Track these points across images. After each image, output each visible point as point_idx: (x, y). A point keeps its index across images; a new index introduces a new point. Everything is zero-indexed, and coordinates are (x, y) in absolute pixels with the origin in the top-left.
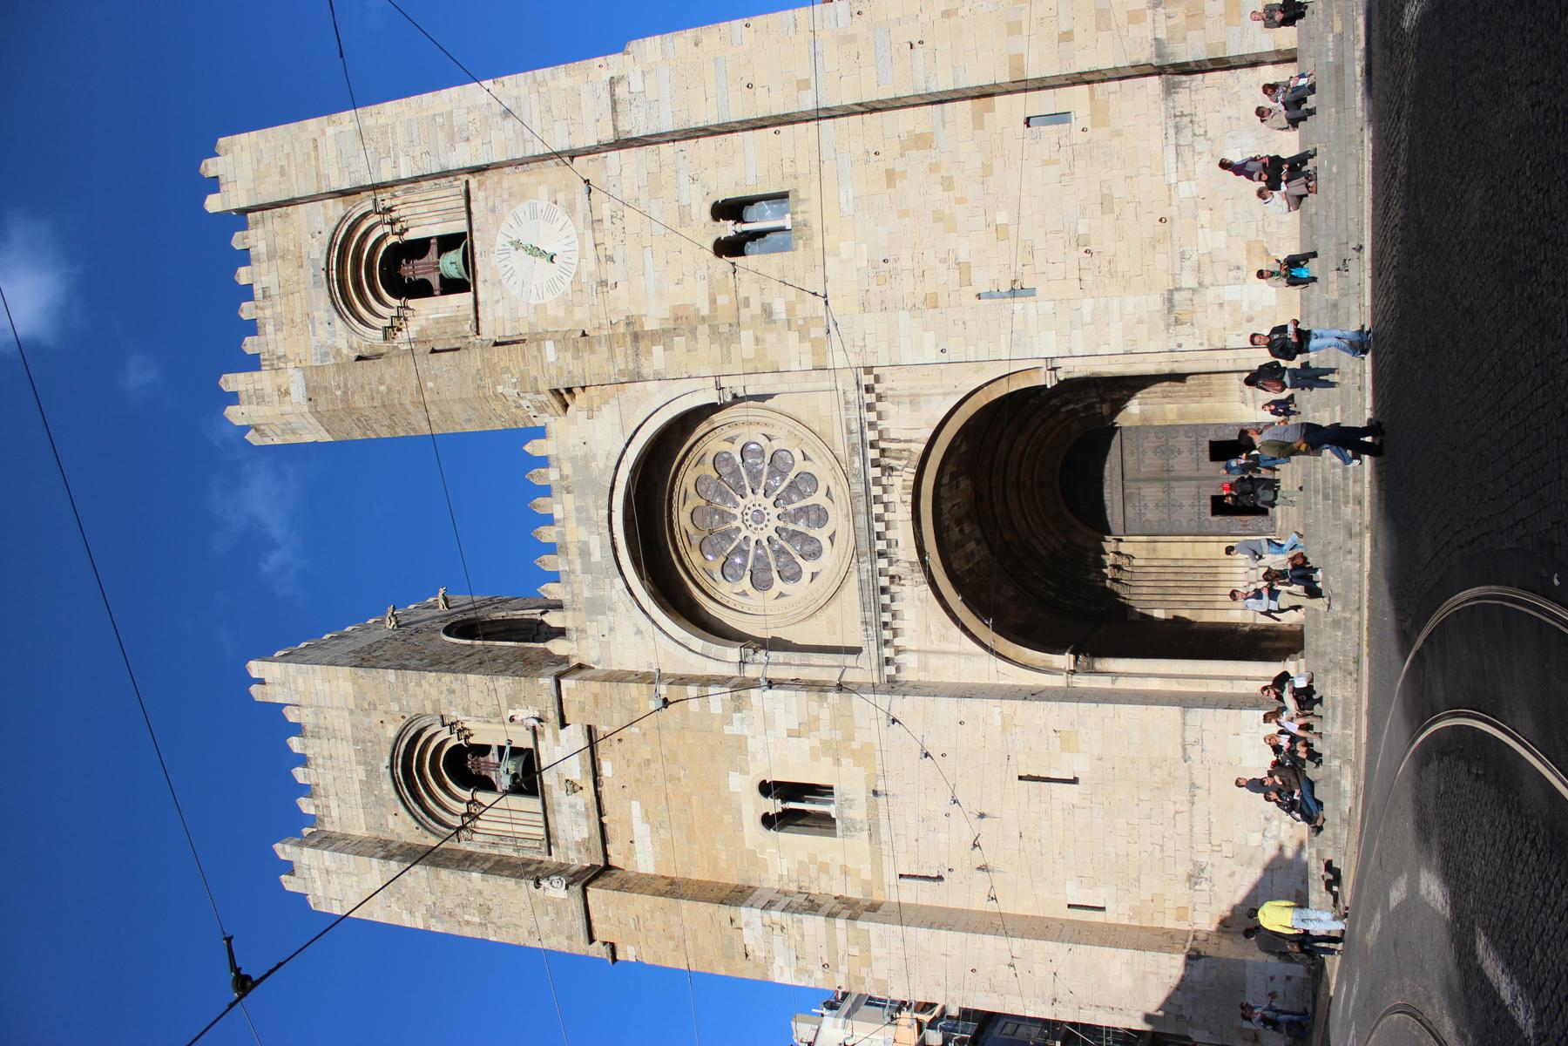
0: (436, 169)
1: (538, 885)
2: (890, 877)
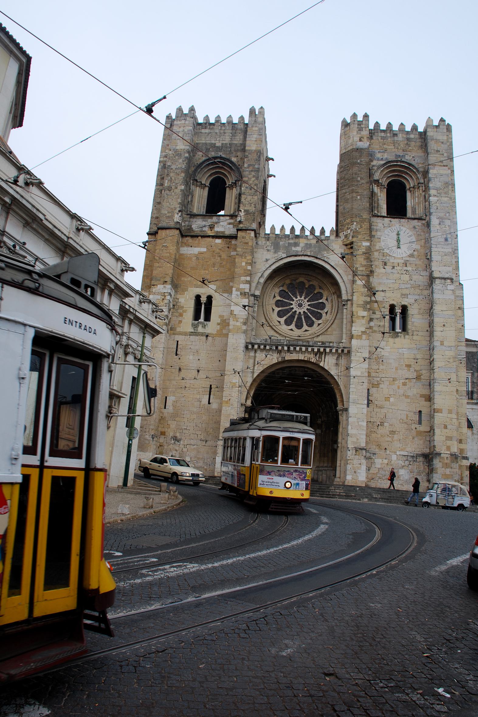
0: (432, 211)
1: (180, 211)
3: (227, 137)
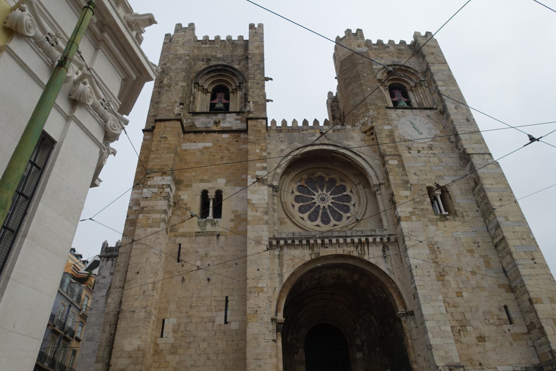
1: (181, 104)
2: (179, 240)
3: (227, 50)
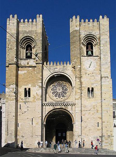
2: (20, 103)
